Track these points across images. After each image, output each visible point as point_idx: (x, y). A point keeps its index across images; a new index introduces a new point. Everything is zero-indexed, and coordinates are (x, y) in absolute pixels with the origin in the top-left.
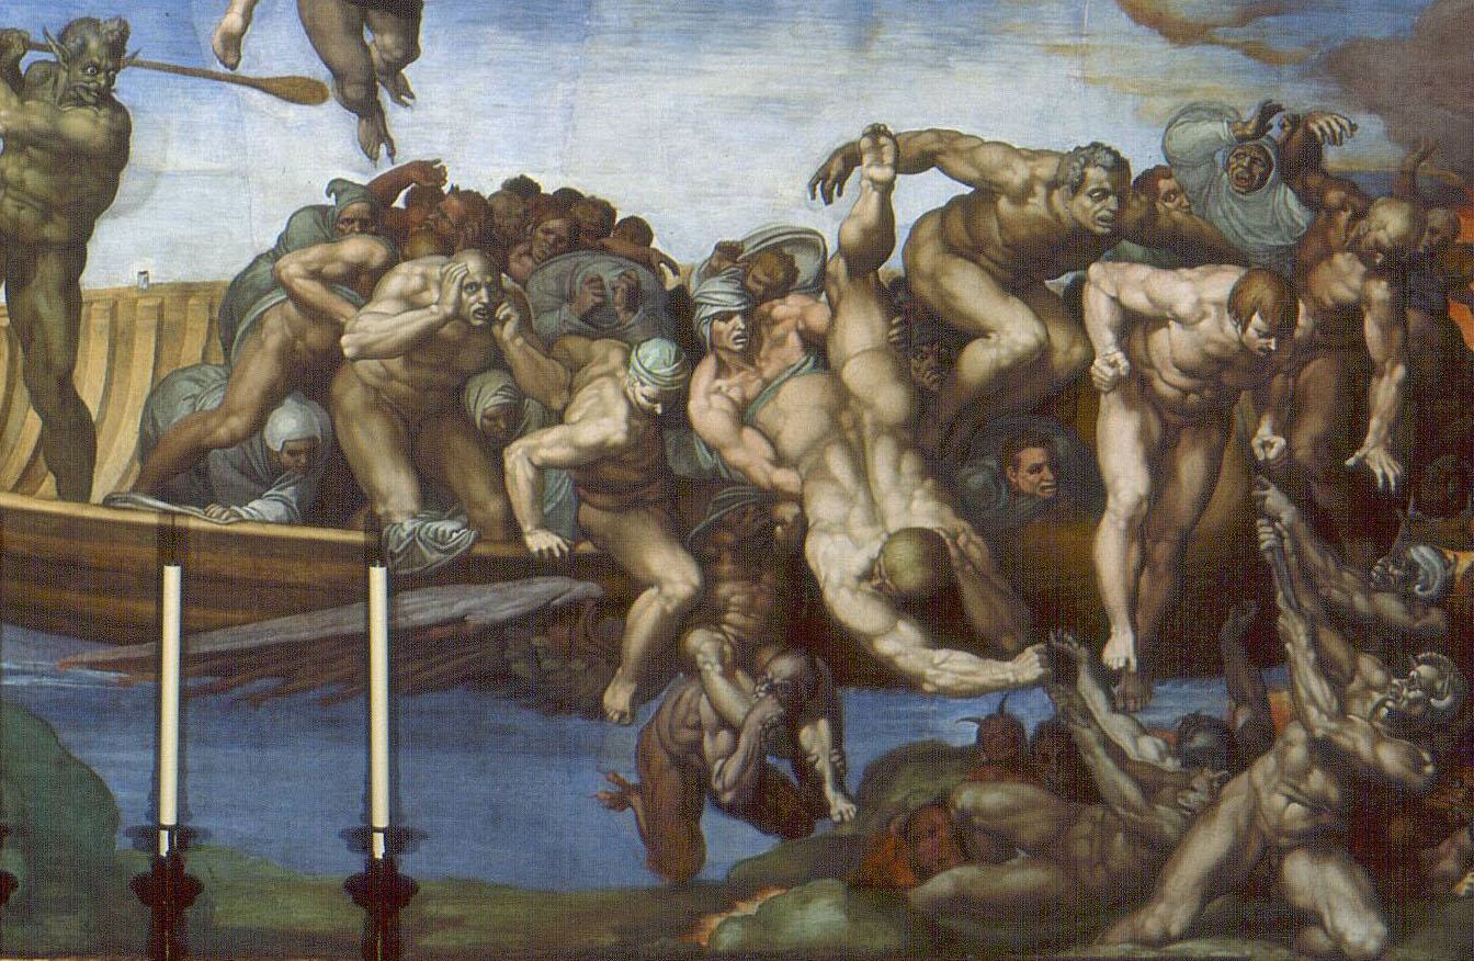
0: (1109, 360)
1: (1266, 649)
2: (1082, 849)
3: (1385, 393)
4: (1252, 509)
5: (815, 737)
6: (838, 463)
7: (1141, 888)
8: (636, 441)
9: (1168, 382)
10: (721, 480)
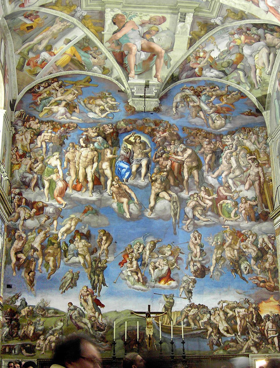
0: (237, 315)
1: (248, 333)
2: (238, 347)
3: (254, 316)
4: (247, 324)
5: (220, 340)
6: (220, 322)
7: (241, 349)
8: (208, 321)
9: (241, 316)
10: (213, 323)
